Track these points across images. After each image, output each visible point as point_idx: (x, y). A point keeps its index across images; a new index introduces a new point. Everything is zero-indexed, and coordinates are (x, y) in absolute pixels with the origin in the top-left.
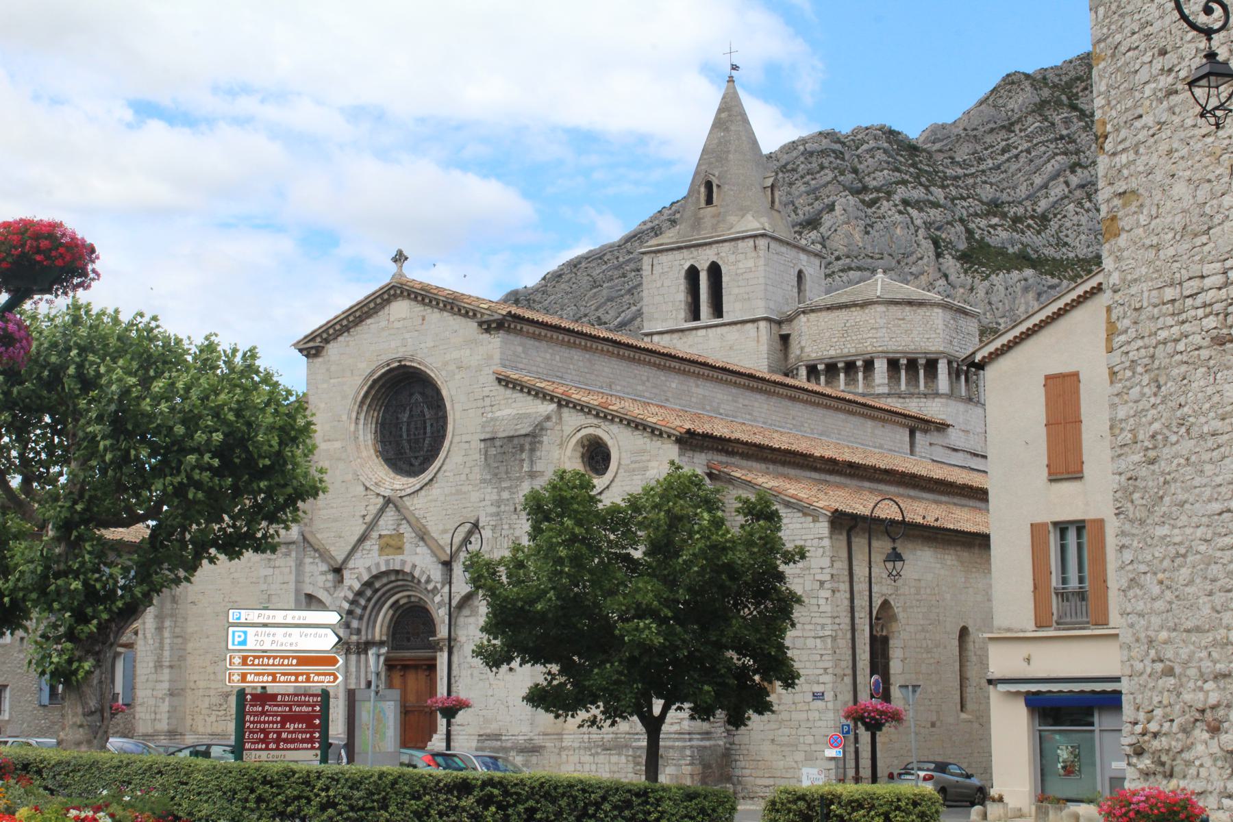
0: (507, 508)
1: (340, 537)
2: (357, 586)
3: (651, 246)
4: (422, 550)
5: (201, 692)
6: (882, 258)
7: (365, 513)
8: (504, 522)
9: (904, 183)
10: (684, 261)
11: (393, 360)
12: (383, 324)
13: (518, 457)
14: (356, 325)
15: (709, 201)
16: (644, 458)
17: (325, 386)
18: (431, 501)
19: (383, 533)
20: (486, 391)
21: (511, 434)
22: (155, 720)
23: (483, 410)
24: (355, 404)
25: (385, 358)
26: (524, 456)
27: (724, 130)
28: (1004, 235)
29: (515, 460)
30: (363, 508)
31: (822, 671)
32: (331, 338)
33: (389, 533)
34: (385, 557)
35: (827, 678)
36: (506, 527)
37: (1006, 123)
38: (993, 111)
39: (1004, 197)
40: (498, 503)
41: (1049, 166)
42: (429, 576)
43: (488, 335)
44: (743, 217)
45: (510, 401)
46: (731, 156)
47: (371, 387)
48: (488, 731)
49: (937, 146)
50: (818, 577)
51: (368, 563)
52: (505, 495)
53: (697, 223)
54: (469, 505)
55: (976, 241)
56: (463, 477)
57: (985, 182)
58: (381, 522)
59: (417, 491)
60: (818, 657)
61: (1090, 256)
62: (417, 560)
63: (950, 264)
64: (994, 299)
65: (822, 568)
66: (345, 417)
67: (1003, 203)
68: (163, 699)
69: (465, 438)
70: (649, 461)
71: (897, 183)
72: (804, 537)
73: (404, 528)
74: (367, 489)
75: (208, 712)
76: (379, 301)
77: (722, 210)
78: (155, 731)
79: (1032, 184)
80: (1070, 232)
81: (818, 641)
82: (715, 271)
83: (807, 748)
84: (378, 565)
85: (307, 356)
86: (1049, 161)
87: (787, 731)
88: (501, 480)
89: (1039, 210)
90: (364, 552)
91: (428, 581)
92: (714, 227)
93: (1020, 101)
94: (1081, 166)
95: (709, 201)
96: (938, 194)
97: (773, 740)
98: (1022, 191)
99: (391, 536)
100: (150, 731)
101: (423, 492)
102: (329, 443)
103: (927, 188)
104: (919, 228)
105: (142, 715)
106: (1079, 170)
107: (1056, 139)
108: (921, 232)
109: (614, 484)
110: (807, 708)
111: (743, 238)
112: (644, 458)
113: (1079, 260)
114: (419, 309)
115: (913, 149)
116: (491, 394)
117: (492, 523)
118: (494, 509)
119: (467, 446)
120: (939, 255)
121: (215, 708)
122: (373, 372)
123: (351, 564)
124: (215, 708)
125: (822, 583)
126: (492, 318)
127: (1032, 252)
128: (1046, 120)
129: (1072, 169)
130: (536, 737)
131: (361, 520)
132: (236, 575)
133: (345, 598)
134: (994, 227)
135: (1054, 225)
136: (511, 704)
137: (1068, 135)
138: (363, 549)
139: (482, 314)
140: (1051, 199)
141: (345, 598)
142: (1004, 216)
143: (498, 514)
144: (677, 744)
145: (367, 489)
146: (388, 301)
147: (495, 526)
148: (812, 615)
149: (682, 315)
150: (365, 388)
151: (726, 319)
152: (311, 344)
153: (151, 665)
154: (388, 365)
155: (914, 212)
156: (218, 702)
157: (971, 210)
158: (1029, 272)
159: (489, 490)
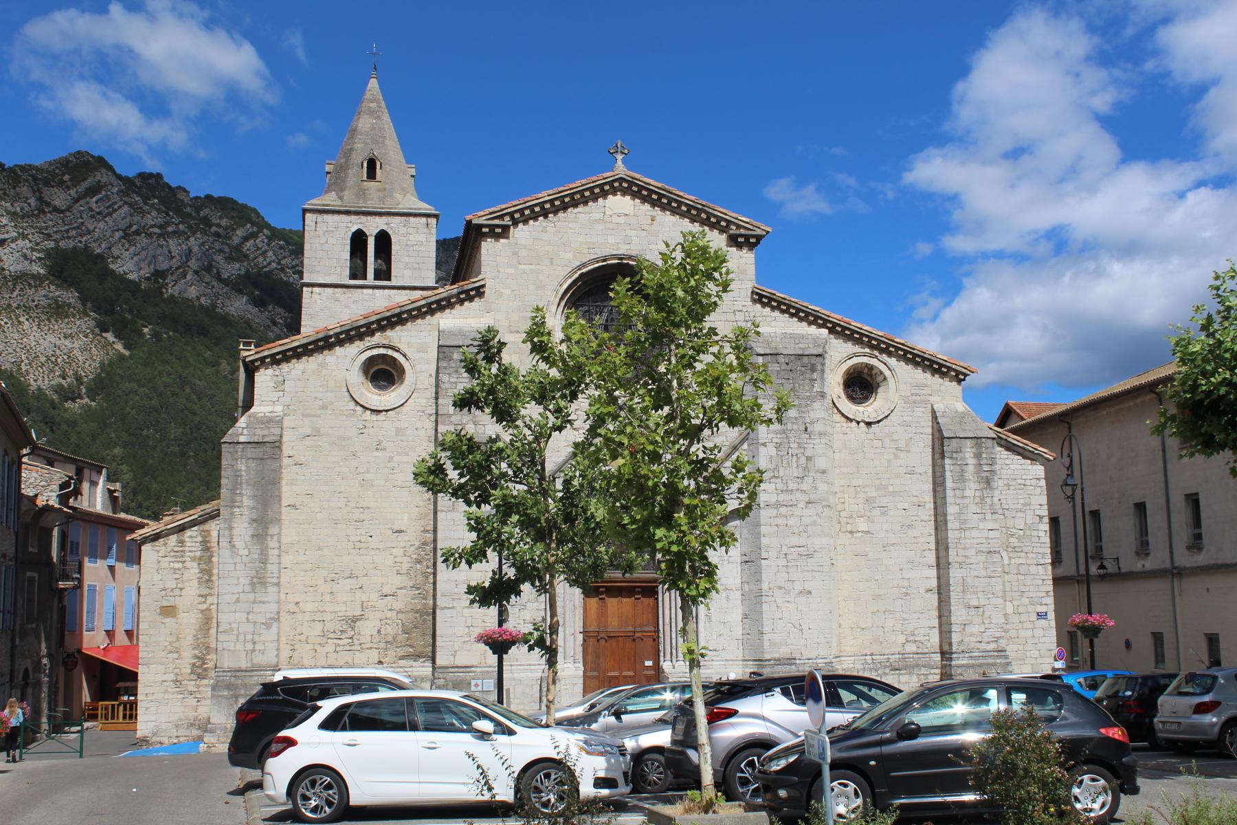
3: (316, 205)
5: (308, 616)
8: (792, 440)
10: (355, 224)
12: (597, 215)
13: (808, 376)
16: (924, 392)
17: (512, 271)
21: (800, 352)
22: (253, 651)
24: (555, 296)
25: (600, 253)
26: (815, 376)
27: (375, 118)
29: (805, 378)
31: (1044, 594)
35: (1050, 600)
36: (795, 445)
44: (405, 196)
45: (769, 319)
46: (387, 142)
47: (574, 282)
48: (777, 656)
50: (1038, 512)
53: (362, 194)
60: (1041, 582)
65: (1041, 505)
68: (268, 626)
70: (931, 395)
72: (1024, 477)
75: (319, 640)
77: (387, 186)
78: (253, 665)
81: (1040, 567)
82: (384, 240)
83: (1033, 661)
87: (1015, 647)
92: (382, 200)
95: (372, 175)
100: (244, 664)
105: (231, 646)
109: (894, 412)
110: (1031, 626)
111: (416, 215)
112: (924, 392)
117: (774, 440)
121: (332, 636)
122: (584, 265)
124: (332, 636)
125: (1041, 517)
126: (750, 233)
130: (834, 660)
132: (367, 477)
136: (805, 627)
139: (738, 227)
144: (998, 661)
146: (604, 194)
147: (781, 444)
148: (1033, 545)
149: (347, 272)
150: (570, 281)
151: (393, 283)
152: (497, 222)
153: (245, 581)
156: (338, 627)
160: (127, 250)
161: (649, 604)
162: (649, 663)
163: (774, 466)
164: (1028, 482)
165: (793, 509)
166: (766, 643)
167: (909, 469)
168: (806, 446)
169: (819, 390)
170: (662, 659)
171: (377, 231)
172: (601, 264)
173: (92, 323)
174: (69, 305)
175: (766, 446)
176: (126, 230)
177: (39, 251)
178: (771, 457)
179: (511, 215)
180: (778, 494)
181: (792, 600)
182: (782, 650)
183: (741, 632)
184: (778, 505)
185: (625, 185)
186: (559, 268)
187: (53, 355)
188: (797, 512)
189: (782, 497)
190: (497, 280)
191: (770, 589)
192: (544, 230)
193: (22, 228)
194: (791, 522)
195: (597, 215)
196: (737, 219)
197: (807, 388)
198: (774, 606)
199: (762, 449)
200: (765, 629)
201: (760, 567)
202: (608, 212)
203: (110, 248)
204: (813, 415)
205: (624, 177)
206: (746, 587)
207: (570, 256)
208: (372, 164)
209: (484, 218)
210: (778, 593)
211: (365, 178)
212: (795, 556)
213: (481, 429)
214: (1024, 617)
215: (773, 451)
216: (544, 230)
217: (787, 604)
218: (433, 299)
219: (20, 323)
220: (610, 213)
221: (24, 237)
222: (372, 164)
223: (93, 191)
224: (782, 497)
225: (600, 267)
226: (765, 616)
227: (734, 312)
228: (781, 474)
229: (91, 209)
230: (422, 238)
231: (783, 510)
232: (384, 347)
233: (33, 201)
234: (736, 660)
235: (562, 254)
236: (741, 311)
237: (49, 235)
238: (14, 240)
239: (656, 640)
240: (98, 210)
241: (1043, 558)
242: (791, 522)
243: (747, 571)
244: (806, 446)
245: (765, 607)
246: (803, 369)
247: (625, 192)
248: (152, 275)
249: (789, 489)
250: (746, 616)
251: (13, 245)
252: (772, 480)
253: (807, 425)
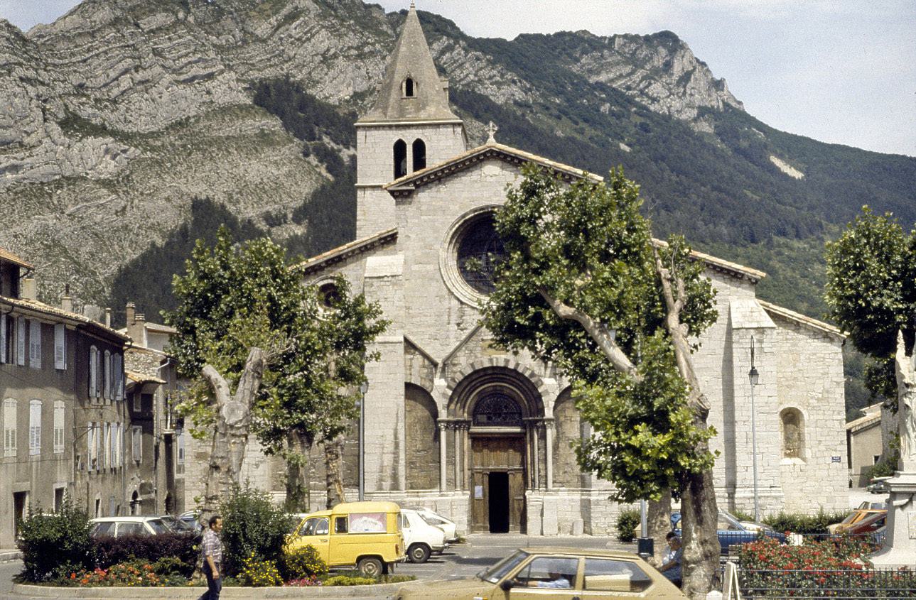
6: (4, 118)
7: (460, 321)
9: (21, 64)
10: (395, 136)
11: (487, 207)
15: (409, 92)
28: (90, 111)
37: (91, 31)
38: (81, 21)
39: (88, 84)
41: (120, 65)
49: (42, 40)
50: (834, 379)
55: (71, 113)
57: (75, 71)
61: (147, 132)
63: (55, 129)
64: (85, 156)
67: (87, 87)
68: (257, 466)
71: (15, 64)
76: (475, 160)
79: (108, 76)
80: (133, 113)
82: (419, 147)
85: (395, 197)
86: (120, 61)
89: (112, 96)
93: (101, 15)
94: (142, 68)
95: (409, 92)
96: (44, 75)
97: (801, 490)
98: (102, 80)
103: (36, 70)
104: (32, 99)
106: (141, 71)
107: (125, 46)
108: (34, 101)
113: (140, 134)
115: (25, 41)
120: (45, 120)
125: (838, 383)
127: (108, 125)
128: (118, 31)
129: (137, 69)
131: (456, 327)
134: (83, 104)
135: (122, 107)
137: (133, 45)
140: (122, 89)
142: (88, 97)
145: (462, 303)
152: (404, 188)
155: (29, 88)
157: (67, 90)
158: (110, 139)
160: (326, 74)
164: (827, 356)
167: (710, 352)
171: (413, 141)
173: (296, 149)
174: (273, 133)
176: (324, 53)
177: (244, 82)
179: (415, 182)
186: (449, 217)
187: (261, 183)
193: (229, 60)
203: (310, 73)
208: (409, 83)
211: (404, 96)
214: (821, 461)
219: (229, 153)
221: (230, 68)
222: (409, 83)
223: (291, 17)
229: (291, 36)
230: (450, 142)
232: (331, 278)
233: (238, 34)
235: (452, 207)
237: (253, 65)
238: (222, 72)
240: (297, 37)
241: (839, 414)
248: (352, 97)
251: (220, 78)
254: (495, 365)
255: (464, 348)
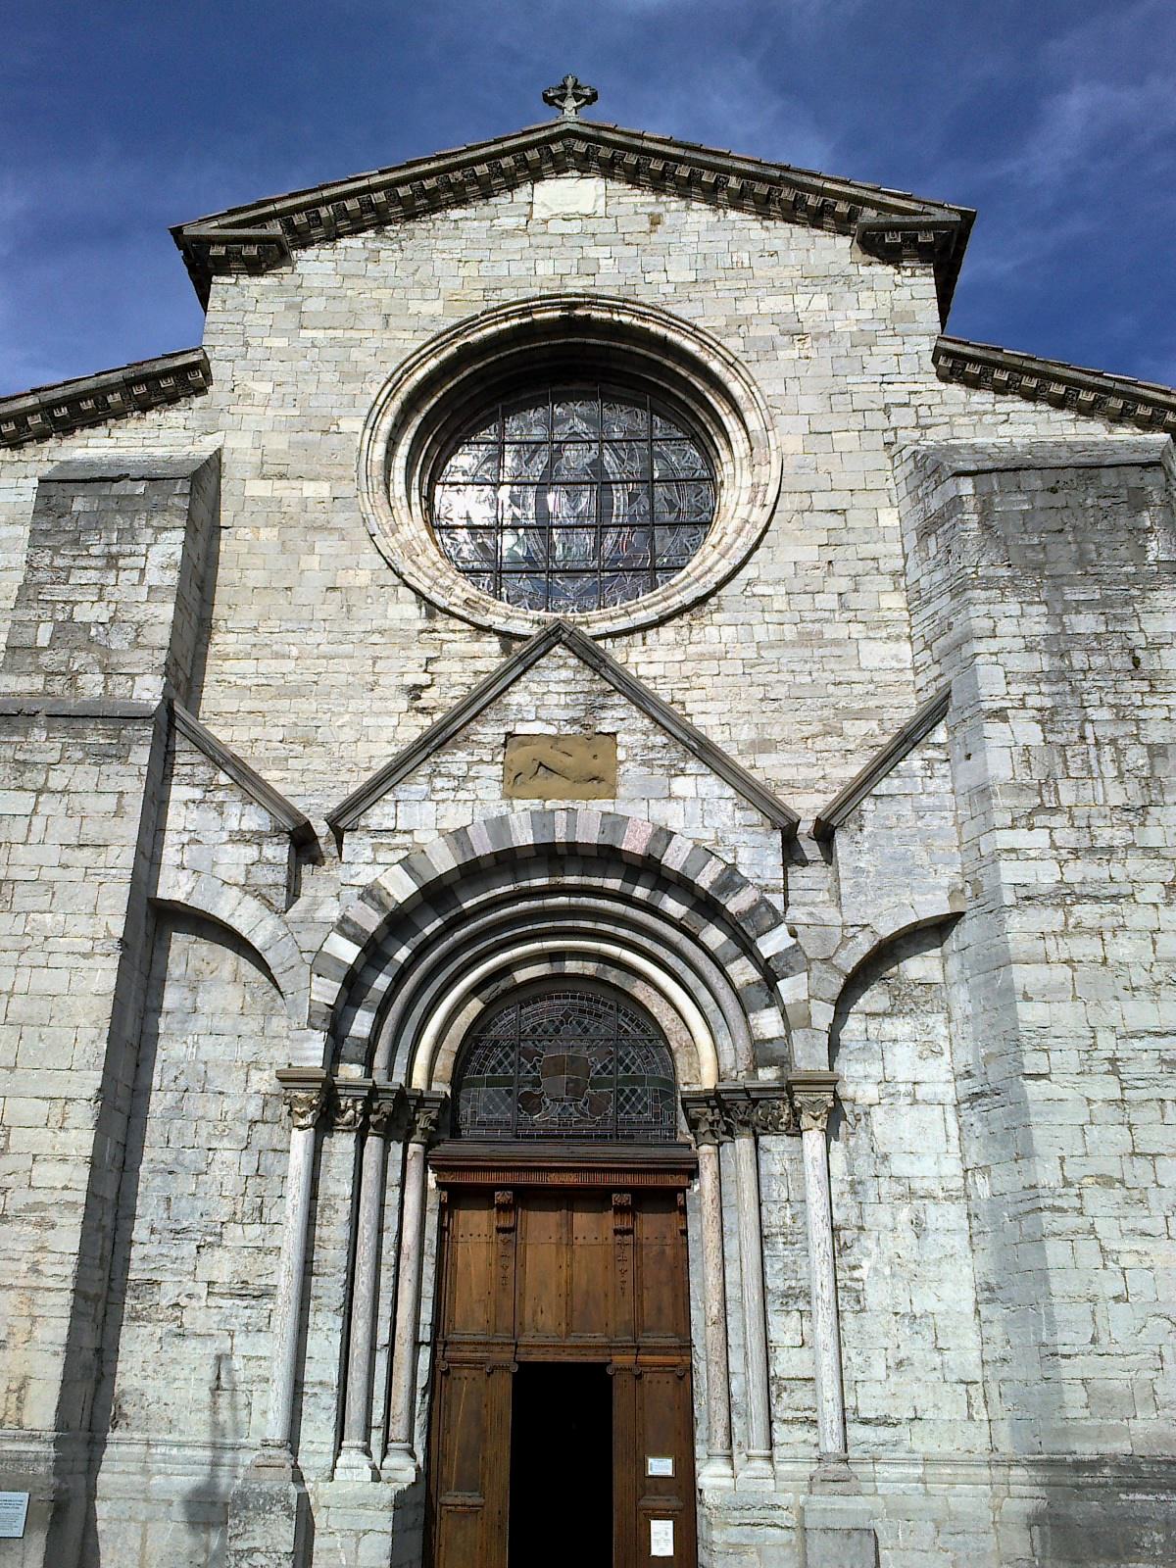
0: (1098, 661)
1: (307, 744)
2: (401, 888)
4: (697, 784)
7: (424, 679)
13: (1122, 521)
14: (411, 216)
18: (701, 658)
19: (521, 729)
20: (897, 393)
23: (890, 436)
29: (1113, 529)
30: (412, 666)
32: (318, 232)
33: (551, 730)
34: (535, 804)
40: (1060, 644)
42: (732, 869)
43: (890, 269)
45: (988, 419)
51: (456, 817)
52: (1086, 623)
54: (855, 676)
56: (829, 601)
58: (517, 697)
59: (644, 628)
62: (672, 816)
66: (353, 424)
69: (821, 501)
73: (620, 719)
74: (431, 608)
84: (500, 824)
88: (1058, 582)
90: (439, 783)
91: (731, 880)
99: (555, 739)
101: (667, 633)
102: (278, 484)
114: (637, 201)
116: (915, 401)
117: (1031, 701)
118: (1042, 662)
119: (835, 521)
122: (470, 324)
123: (379, 815)
131: (403, 703)
133: (345, 927)
138: (435, 774)
141: (345, 927)
143: (1061, 676)
145: (431, 608)
147: (1054, 711)
154: (526, 312)
159: (1013, 608)
161: (663, 1252)
162: (660, 1466)
163: (1038, 775)
165: (1124, 907)
166: (1076, 1396)
168: (1142, 714)
169: (1163, 557)
170: (700, 1450)
172: (515, 322)
175: (1005, 720)
178: (1027, 748)
180: (1062, 864)
181: (1156, 1225)
182: (1137, 1425)
183: (974, 1356)
184: (1065, 896)
185: (581, 147)
186: (408, 335)
188: (1139, 918)
189: (1075, 872)
190: (240, 363)
191: (1067, 1183)
192: (374, 257)
194: (1123, 949)
195: (513, 220)
196: (877, 191)
197: (1123, 552)
198: (1088, 1249)
199: (994, 729)
200: (1068, 1338)
201: (1020, 1105)
202: (539, 213)
204: (1153, 626)
205: (576, 127)
206: (983, 1187)
207: (437, 307)
209: (215, 224)
210: (1099, 1201)
212: (1147, 1065)
213: (120, 688)
215: (1031, 734)
216: (374, 257)
217: (1141, 1245)
218: (58, 394)
220: (546, 216)
224: (1075, 872)
225: (513, 329)
226: (1056, 1285)
227: (886, 409)
228: (1067, 797)
231: (1087, 913)
234: (969, 1464)
236: (906, 405)
239: (684, 1376)
242: (1123, 949)
243: (978, 1128)
244: (1142, 714)
245: (1056, 1252)
246: (1104, 503)
247: (584, 165)
249: (1100, 843)
250: (989, 1292)
252: (1038, 820)
253: (1139, 653)
254: (560, 836)
255: (425, 769)
